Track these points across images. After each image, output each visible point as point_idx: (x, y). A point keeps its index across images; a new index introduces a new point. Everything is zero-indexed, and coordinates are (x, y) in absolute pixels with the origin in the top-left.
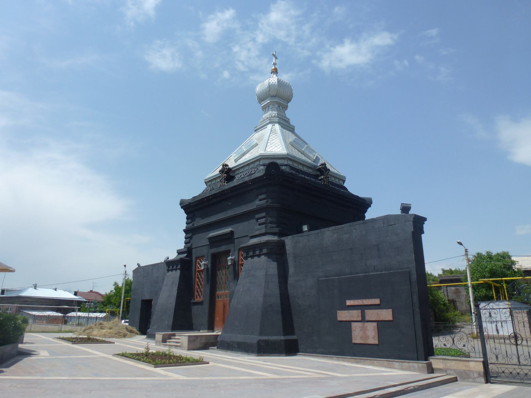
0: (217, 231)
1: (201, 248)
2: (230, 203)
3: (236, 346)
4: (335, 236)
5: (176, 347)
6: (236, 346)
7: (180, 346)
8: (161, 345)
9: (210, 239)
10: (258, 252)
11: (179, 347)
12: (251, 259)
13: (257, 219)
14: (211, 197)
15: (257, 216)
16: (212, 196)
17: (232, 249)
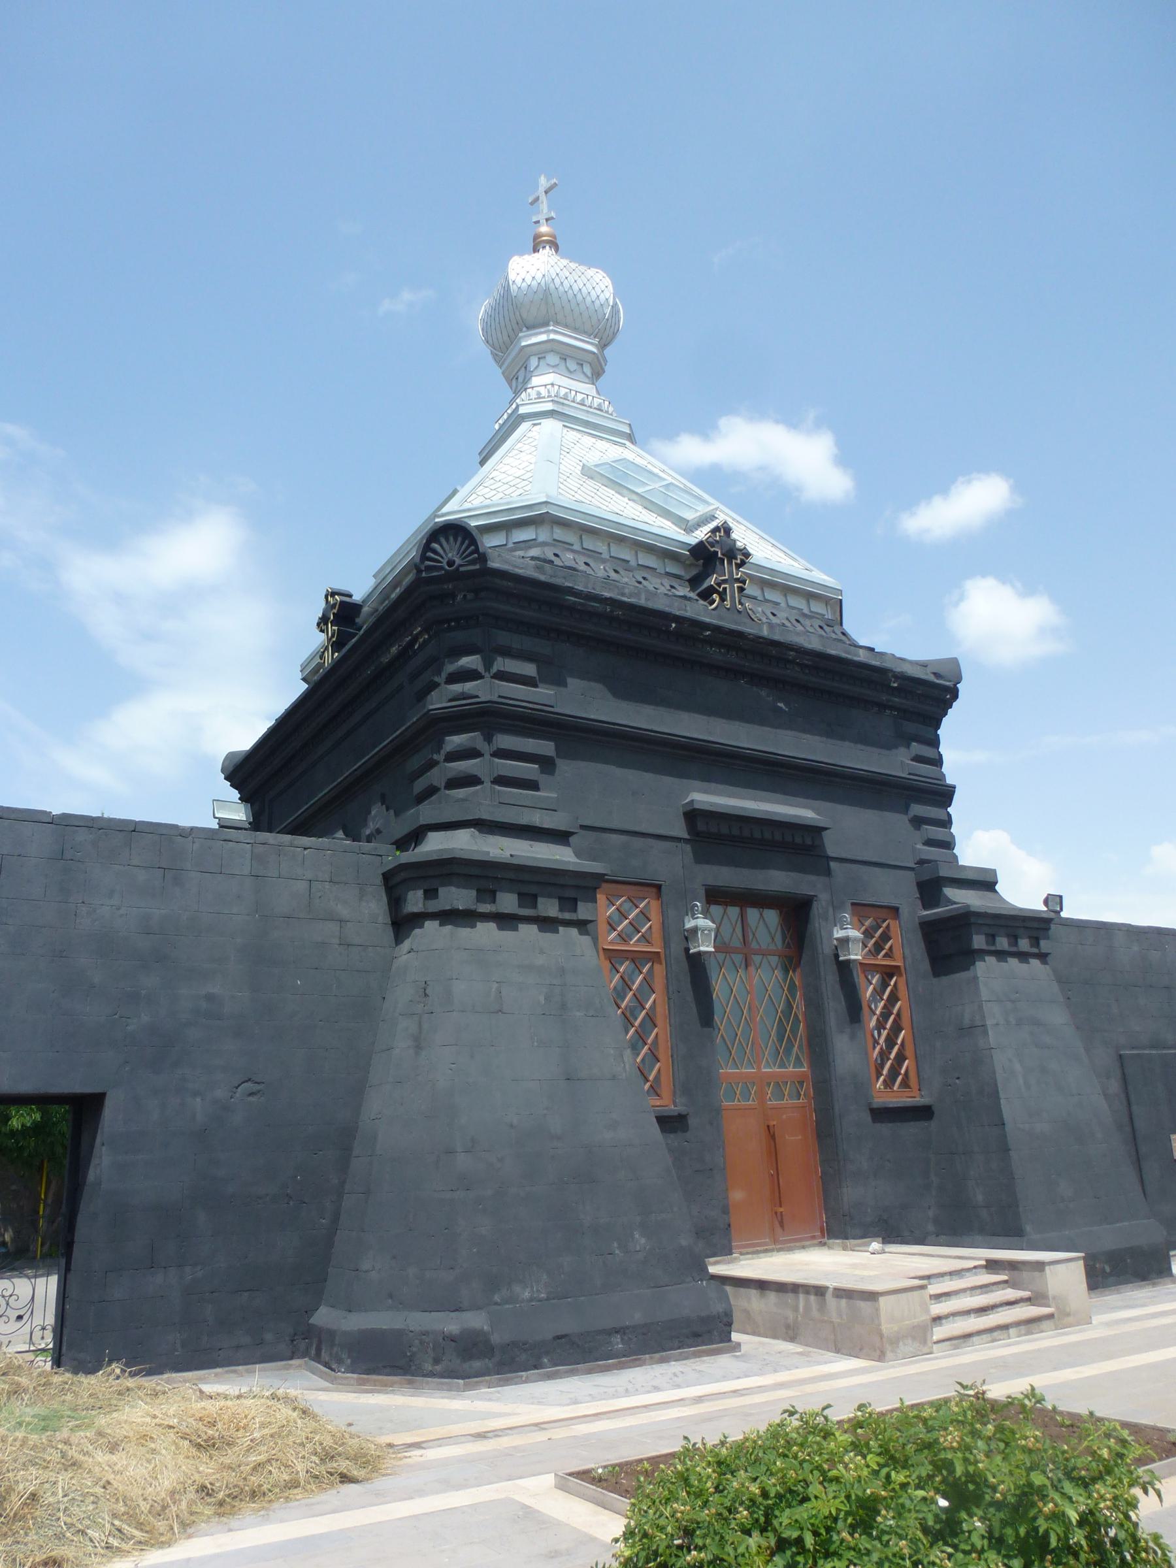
0: (719, 794)
1: (638, 842)
2: (781, 705)
3: (1108, 1269)
4: (1136, 948)
5: (1034, 1326)
6: (1108, 1269)
7: (1050, 1316)
8: (935, 1346)
9: (693, 816)
10: (1024, 944)
11: (1045, 1324)
12: (441, 925)
13: (918, 822)
14: (708, 633)
15: (918, 809)
16: (717, 629)
17: (823, 898)
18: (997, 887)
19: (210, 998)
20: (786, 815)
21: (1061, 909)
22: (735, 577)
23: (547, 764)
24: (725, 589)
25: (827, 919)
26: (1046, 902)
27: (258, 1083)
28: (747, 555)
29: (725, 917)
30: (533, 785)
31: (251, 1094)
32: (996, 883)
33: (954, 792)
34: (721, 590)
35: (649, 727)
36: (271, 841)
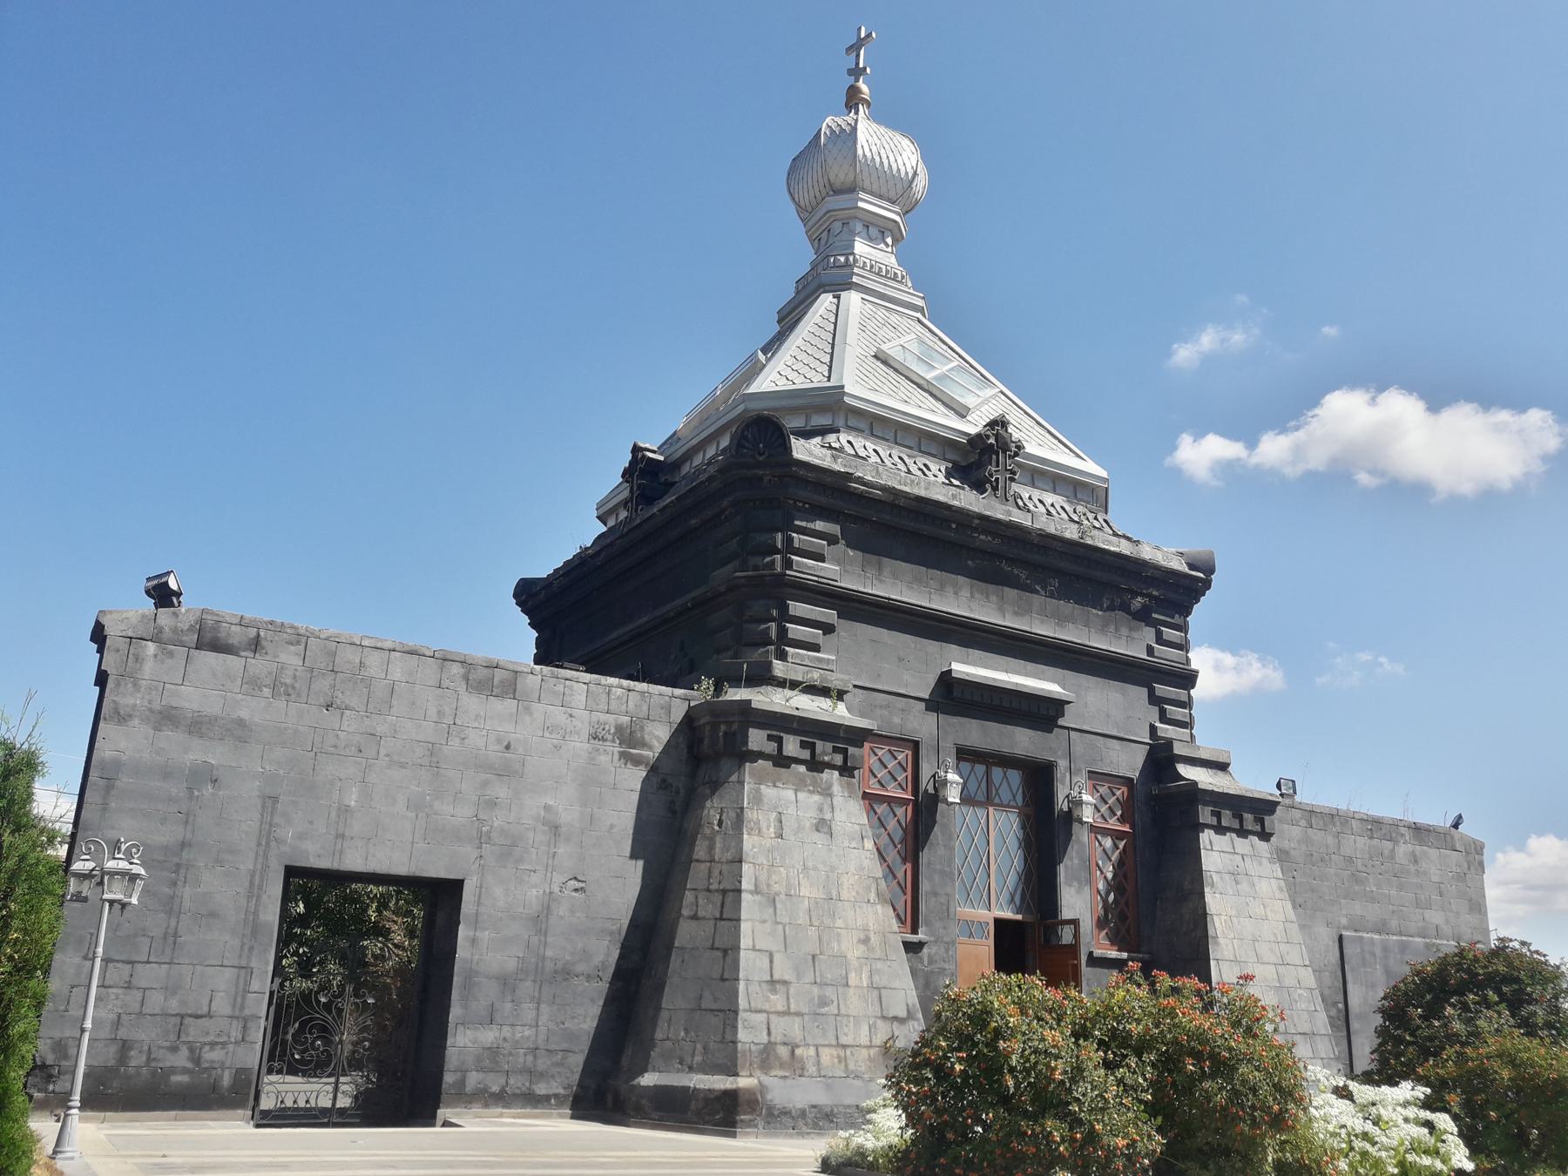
15: (1162, 690)
17: (1062, 764)
18: (1230, 769)
19: (547, 808)
20: (1034, 688)
21: (1295, 792)
22: (1008, 468)
23: (828, 629)
24: (997, 479)
25: (1064, 784)
26: (1279, 786)
27: (582, 881)
28: (1020, 447)
29: (972, 773)
30: (815, 648)
31: (576, 890)
32: (1229, 764)
33: (1197, 676)
34: (993, 480)
35: (919, 603)
36: (603, 682)
